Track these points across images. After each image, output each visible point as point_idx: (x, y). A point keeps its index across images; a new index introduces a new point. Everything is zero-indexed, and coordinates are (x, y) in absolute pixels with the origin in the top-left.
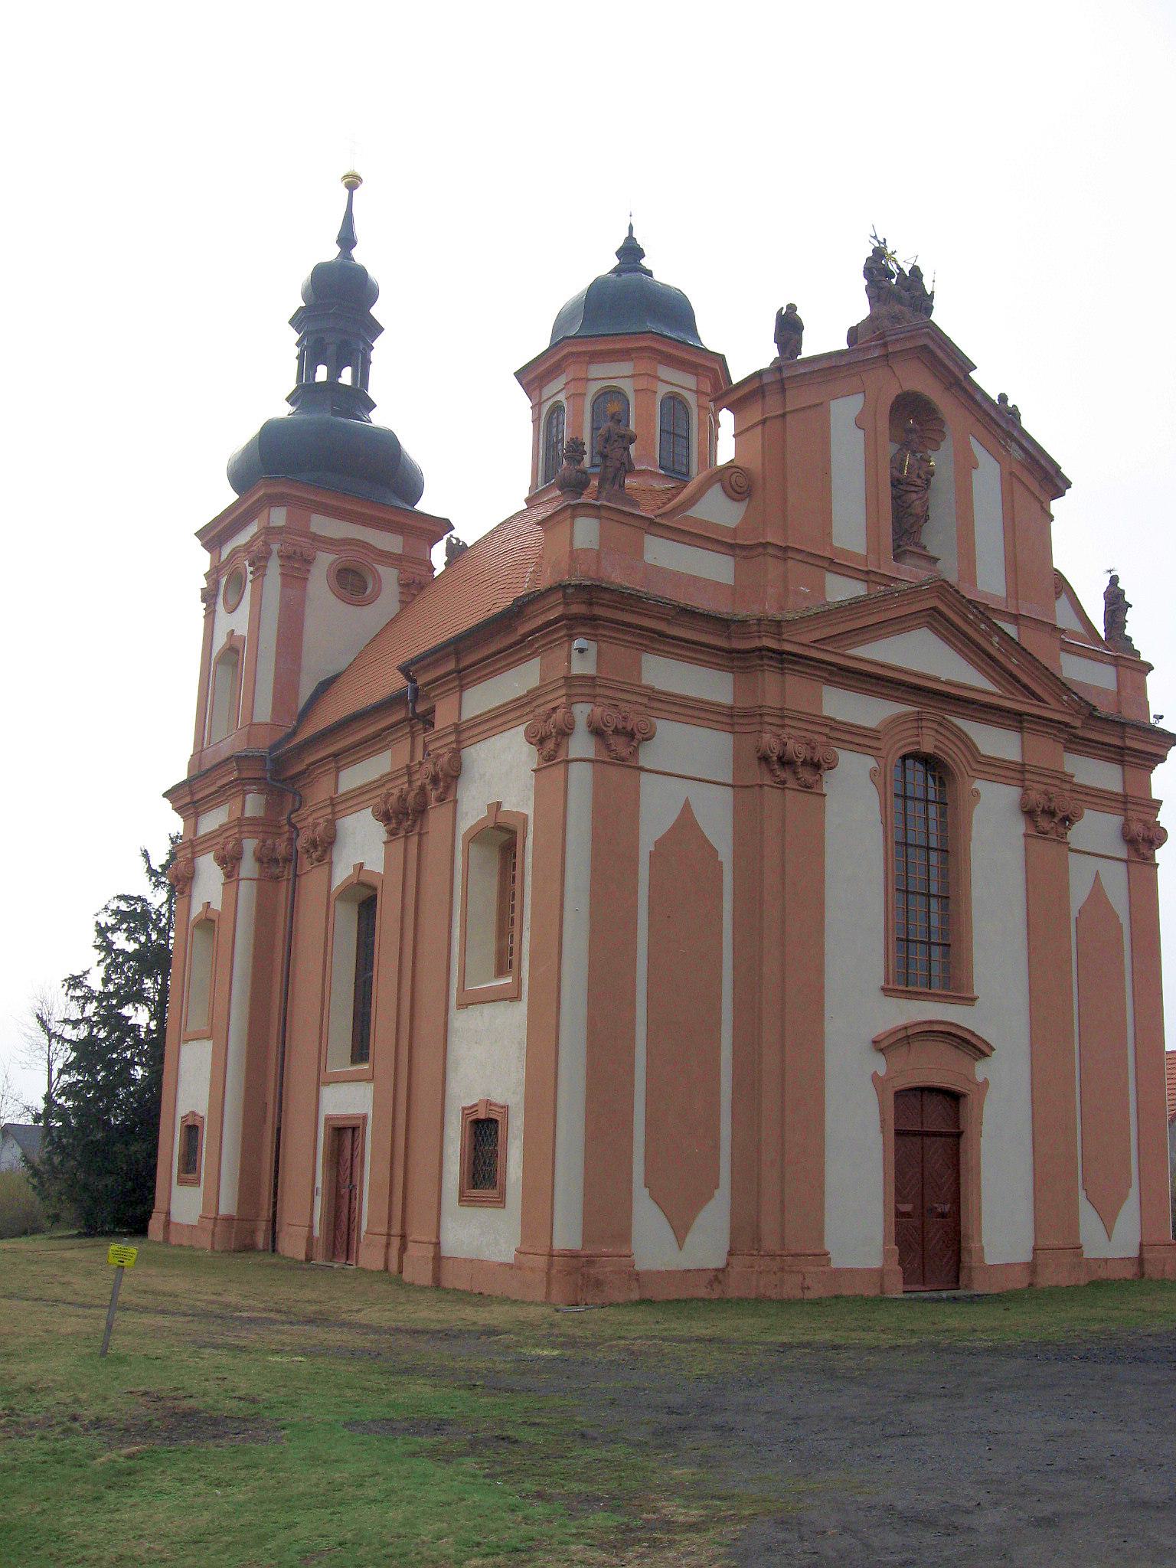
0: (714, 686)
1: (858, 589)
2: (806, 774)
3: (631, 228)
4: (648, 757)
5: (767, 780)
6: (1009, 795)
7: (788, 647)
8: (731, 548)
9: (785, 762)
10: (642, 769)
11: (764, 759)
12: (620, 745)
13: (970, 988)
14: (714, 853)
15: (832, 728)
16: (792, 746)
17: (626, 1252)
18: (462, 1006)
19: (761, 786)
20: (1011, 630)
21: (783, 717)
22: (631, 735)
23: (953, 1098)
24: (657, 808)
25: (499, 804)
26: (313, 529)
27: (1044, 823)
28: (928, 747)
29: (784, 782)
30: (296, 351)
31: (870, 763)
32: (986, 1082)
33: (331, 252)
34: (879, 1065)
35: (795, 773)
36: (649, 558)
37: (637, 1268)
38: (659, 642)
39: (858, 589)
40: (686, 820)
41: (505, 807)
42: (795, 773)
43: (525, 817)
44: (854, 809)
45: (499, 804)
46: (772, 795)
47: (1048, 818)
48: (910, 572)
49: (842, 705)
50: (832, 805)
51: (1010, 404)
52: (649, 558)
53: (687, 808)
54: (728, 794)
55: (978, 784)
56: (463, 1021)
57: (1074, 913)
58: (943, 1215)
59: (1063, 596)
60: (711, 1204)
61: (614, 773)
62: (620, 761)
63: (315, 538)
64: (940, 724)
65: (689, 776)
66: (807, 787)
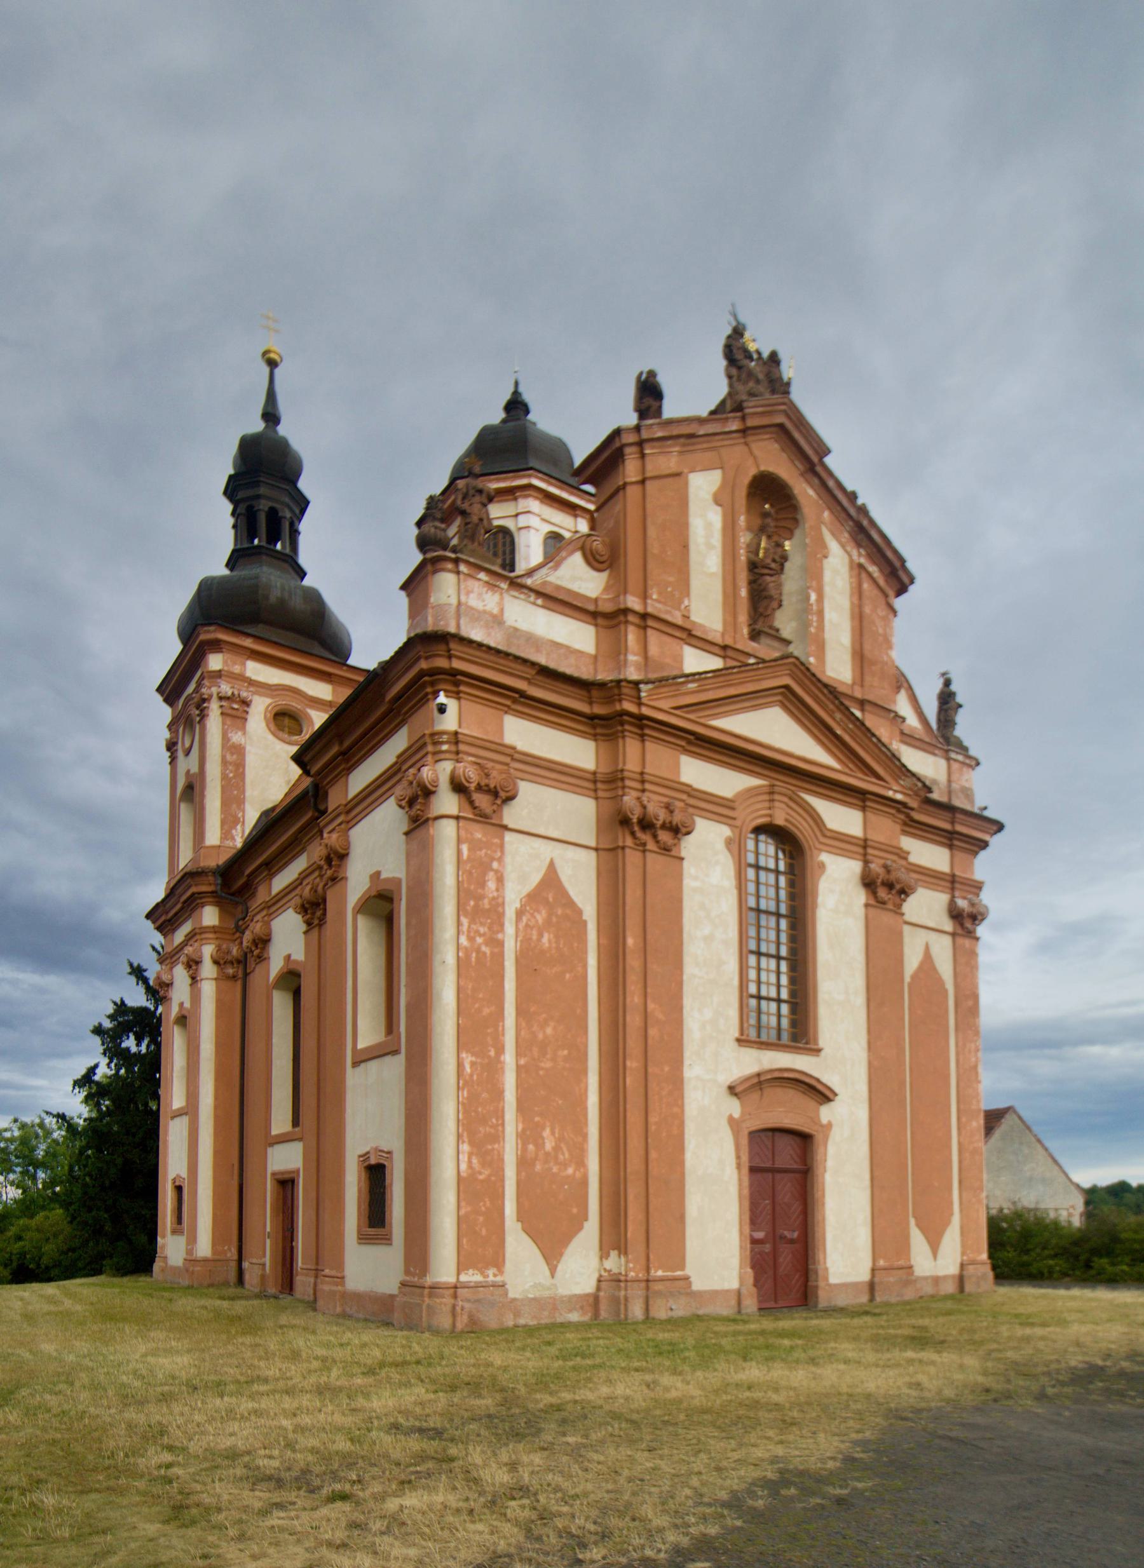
2: (665, 836)
5: (629, 841)
9: (646, 824)
10: (506, 828)
11: (625, 822)
14: (580, 912)
15: (689, 795)
16: (652, 808)
17: (499, 1279)
18: (355, 1064)
19: (623, 848)
21: (643, 782)
24: (521, 865)
25: (378, 873)
26: (249, 674)
29: (644, 844)
30: (232, 521)
35: (655, 836)
37: (511, 1295)
40: (551, 878)
41: (384, 876)
42: (655, 836)
43: (399, 880)
44: (710, 874)
45: (378, 873)
46: (632, 857)
49: (698, 773)
50: (689, 869)
53: (552, 865)
54: (593, 855)
56: (354, 1078)
60: (581, 1235)
63: (251, 683)
64: (791, 798)
65: (550, 839)
66: (666, 850)
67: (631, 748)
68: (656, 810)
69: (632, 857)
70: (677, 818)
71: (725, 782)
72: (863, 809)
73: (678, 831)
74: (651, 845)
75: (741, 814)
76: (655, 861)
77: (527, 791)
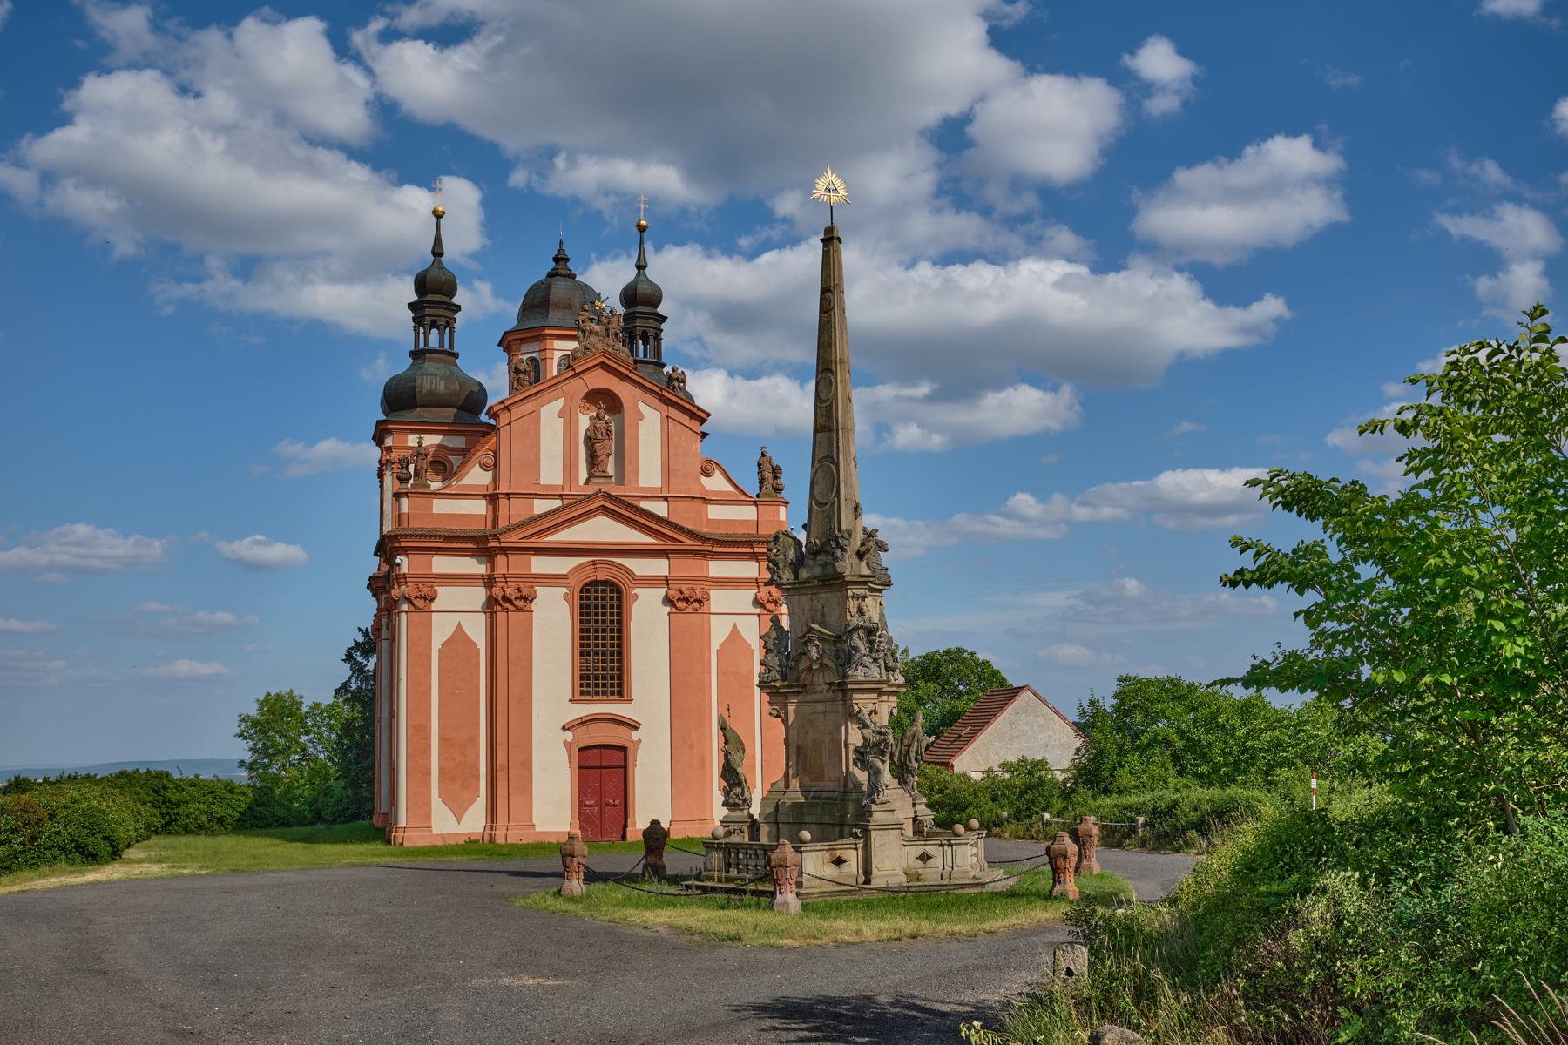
0: (472, 566)
1: (557, 503)
2: (519, 603)
4: (434, 606)
6: (662, 592)
8: (484, 496)
9: (506, 599)
12: (420, 603)
20: (660, 508)
22: (425, 598)
23: (624, 749)
27: (681, 605)
28: (602, 577)
31: (565, 590)
34: (569, 736)
36: (435, 510)
38: (439, 551)
39: (557, 503)
47: (686, 602)
48: (590, 490)
49: (540, 565)
52: (435, 510)
55: (637, 591)
57: (715, 646)
61: (417, 616)
62: (419, 610)
66: (519, 609)
67: (501, 560)
68: (511, 592)
69: (501, 617)
70: (525, 592)
73: (528, 599)
74: (511, 608)
77: (442, 591)
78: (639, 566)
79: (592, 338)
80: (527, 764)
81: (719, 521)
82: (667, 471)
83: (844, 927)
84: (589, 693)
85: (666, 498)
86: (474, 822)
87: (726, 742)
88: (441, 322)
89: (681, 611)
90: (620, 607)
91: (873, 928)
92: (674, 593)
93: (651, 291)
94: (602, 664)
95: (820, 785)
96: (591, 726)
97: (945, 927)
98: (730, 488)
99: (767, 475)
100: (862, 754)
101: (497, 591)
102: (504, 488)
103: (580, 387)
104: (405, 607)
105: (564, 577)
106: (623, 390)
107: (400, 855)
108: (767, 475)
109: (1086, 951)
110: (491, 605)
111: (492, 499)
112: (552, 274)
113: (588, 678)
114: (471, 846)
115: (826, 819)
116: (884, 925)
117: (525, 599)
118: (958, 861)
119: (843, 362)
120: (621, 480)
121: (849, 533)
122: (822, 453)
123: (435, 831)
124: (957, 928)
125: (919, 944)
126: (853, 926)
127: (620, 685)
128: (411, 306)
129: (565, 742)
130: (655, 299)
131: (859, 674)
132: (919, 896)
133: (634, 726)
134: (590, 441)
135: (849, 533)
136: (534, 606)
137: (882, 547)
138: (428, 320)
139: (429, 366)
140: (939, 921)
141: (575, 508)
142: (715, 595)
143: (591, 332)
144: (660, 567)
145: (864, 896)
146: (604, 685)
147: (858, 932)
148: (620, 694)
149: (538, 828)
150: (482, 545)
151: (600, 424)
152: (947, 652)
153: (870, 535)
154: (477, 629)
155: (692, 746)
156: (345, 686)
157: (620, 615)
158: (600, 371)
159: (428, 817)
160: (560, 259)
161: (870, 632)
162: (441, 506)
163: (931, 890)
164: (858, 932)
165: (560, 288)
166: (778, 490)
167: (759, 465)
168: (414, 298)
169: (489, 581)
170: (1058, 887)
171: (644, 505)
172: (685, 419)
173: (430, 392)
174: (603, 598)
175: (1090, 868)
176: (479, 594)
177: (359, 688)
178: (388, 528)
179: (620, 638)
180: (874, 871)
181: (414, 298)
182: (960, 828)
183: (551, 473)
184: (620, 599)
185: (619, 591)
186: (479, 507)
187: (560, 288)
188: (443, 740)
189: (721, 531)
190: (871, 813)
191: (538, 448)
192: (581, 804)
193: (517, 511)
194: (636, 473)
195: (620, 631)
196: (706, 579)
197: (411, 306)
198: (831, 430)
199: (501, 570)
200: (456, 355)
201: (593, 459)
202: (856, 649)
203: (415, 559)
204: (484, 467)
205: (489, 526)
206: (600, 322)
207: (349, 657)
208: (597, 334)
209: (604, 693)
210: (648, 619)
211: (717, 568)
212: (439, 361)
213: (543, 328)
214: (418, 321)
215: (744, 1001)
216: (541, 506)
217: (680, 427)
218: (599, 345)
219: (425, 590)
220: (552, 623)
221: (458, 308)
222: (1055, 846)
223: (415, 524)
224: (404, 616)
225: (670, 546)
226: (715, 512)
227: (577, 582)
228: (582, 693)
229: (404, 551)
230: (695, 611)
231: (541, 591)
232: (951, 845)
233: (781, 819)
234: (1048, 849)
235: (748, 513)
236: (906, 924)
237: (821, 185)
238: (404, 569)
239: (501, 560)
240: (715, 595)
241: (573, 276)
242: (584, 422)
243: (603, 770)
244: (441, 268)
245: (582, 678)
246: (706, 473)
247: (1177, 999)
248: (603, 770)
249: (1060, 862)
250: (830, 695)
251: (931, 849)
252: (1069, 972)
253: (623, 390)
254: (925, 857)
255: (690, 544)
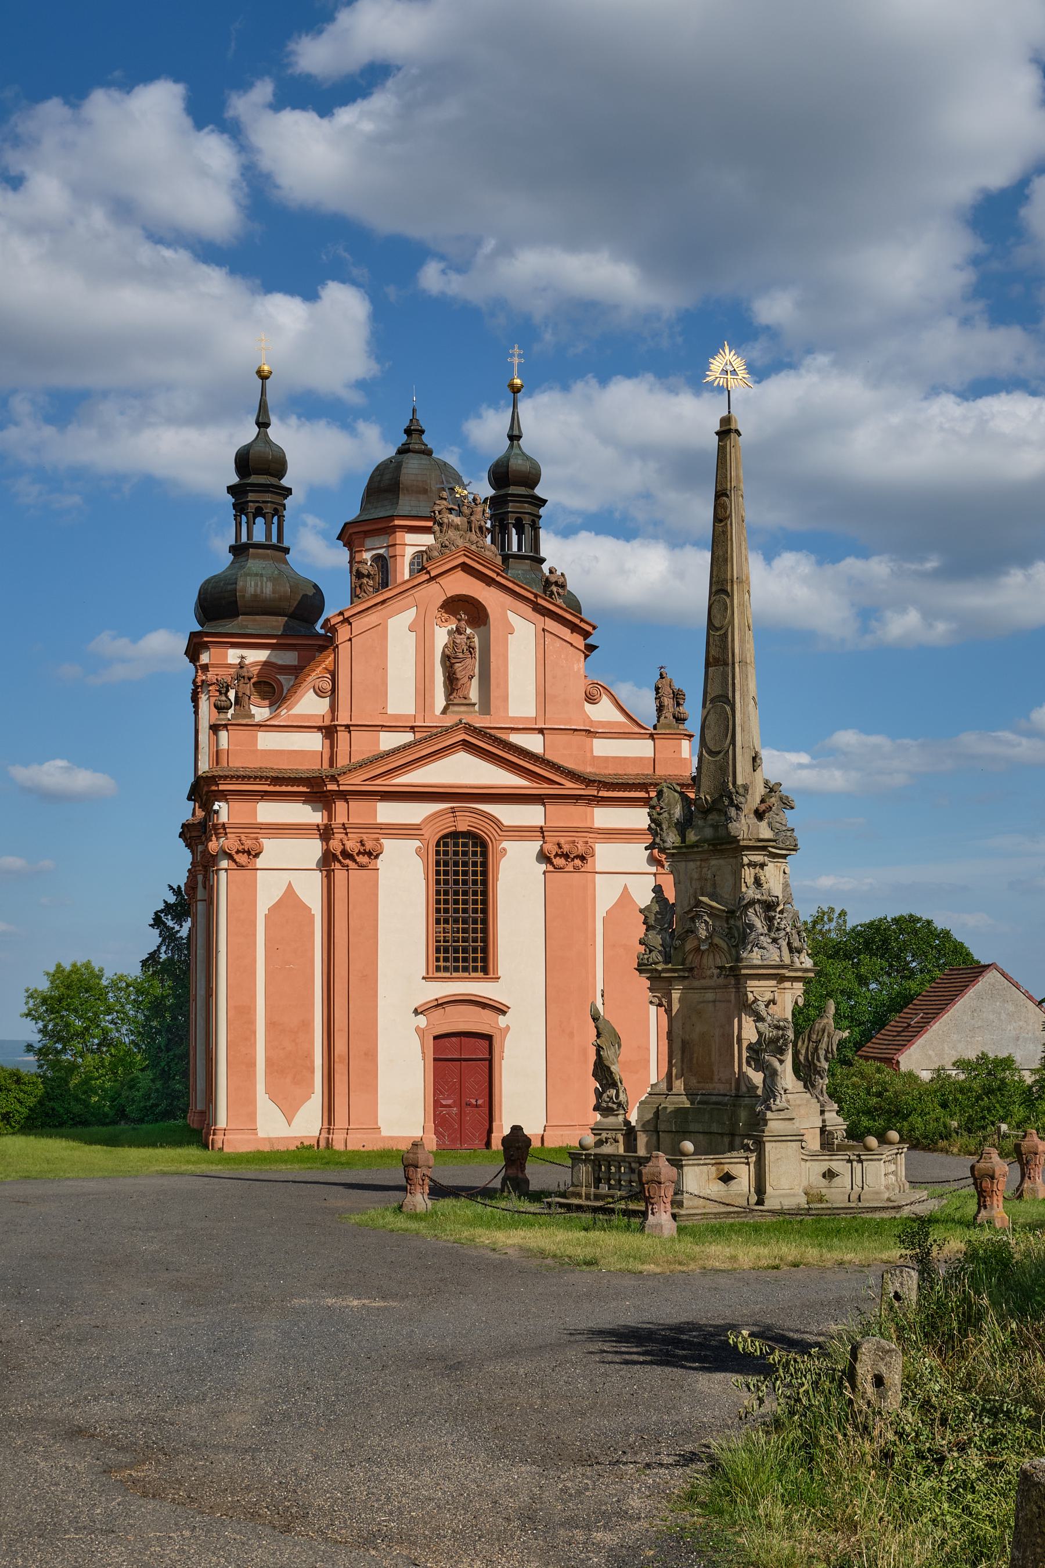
1: (408, 737)
2: (363, 859)
3: (414, 411)
4: (260, 863)
7: (342, 788)
8: (319, 728)
9: (346, 854)
12: (242, 859)
13: (495, 971)
20: (533, 743)
22: (249, 853)
23: (489, 1038)
24: (268, 890)
27: (560, 862)
28: (463, 827)
32: (508, 1028)
33: (248, 433)
34: (422, 1021)
36: (261, 746)
39: (408, 737)
42: (355, 861)
47: (564, 857)
48: (449, 721)
49: (388, 812)
51: (559, 573)
52: (261, 746)
55: (505, 844)
57: (601, 912)
58: (477, 1106)
59: (604, 697)
62: (241, 867)
66: (362, 867)
67: (340, 806)
68: (352, 845)
69: (340, 875)
70: (369, 845)
71: (415, 813)
72: (544, 804)
73: (373, 855)
74: (352, 865)
75: (427, 832)
76: (356, 875)
78: (508, 814)
79: (451, 533)
80: (371, 1055)
81: (606, 759)
82: (543, 697)
83: (718, 1253)
84: (446, 969)
85: (541, 731)
86: (307, 1124)
87: (598, 1036)
88: (268, 509)
89: (558, 869)
90: (484, 864)
91: (749, 1254)
92: (551, 848)
93: (526, 467)
94: (463, 935)
95: (709, 1087)
96: (449, 1009)
97: (832, 1256)
98: (621, 718)
99: (668, 701)
100: (757, 1052)
101: (335, 845)
102: (343, 719)
103: (435, 594)
104: (224, 864)
105: (417, 827)
106: (489, 597)
107: (220, 1161)
108: (668, 701)
109: (914, 1274)
110: (327, 861)
111: (329, 732)
112: (403, 451)
113: (446, 951)
114: (303, 1153)
115: (715, 1128)
116: (764, 1251)
117: (369, 854)
118: (870, 1180)
119: (740, 581)
120: (485, 706)
121: (746, 788)
122: (715, 691)
123: (261, 1134)
124: (849, 1257)
125: (800, 1274)
126: (728, 1251)
127: (485, 960)
128: (231, 489)
129: (417, 1029)
130: (532, 479)
131: (755, 957)
132: (817, 1220)
133: (501, 1010)
134: (449, 661)
135: (746, 788)
136: (380, 863)
137: (787, 804)
138: (251, 508)
139: (254, 565)
140: (830, 1249)
141: (430, 744)
142: (600, 849)
143: (450, 525)
144: (532, 815)
145: (756, 1219)
146: (465, 960)
147: (734, 1258)
148: (485, 970)
149: (385, 1133)
150: (317, 789)
151: (461, 639)
152: (896, 921)
153: (772, 789)
154: (310, 890)
155: (571, 1035)
156: (153, 956)
157: (485, 873)
158: (460, 574)
159: (252, 1116)
160: (413, 431)
161: (769, 906)
162: (267, 741)
163: (834, 1212)
164: (734, 1258)
165: (413, 465)
166: (680, 719)
167: (657, 689)
168: (235, 479)
169: (325, 833)
170: (983, 1213)
171: (515, 739)
172: (565, 633)
173: (255, 596)
174: (465, 853)
175: (1034, 1191)
176: (314, 848)
177: (170, 960)
178: (204, 767)
179: (485, 902)
180: (769, 1190)
181: (235, 479)
182: (872, 1141)
183: (401, 701)
184: (484, 854)
185: (484, 845)
186: (314, 742)
187: (413, 465)
188: (270, 1025)
189: (608, 772)
190: (765, 1122)
191: (385, 669)
192: (437, 1104)
193: (356, 747)
194: (505, 699)
195: (485, 893)
196: (591, 830)
197: (231, 489)
198: (726, 664)
199: (340, 818)
200: (287, 551)
201: (452, 682)
202: (751, 927)
203: (237, 806)
204: (319, 693)
205: (326, 765)
206: (460, 513)
207: (157, 921)
208: (457, 528)
209: (465, 969)
210: (518, 881)
211: (605, 817)
212: (265, 557)
213: (392, 518)
214: (240, 508)
215: (582, 1326)
216: (388, 741)
217: (559, 643)
218: (460, 542)
219: (248, 844)
220: (402, 885)
221: (288, 491)
222: (981, 1165)
223: (237, 763)
224: (223, 875)
225: (545, 789)
226: (602, 748)
227: (433, 834)
228: (438, 969)
229: (223, 796)
230: (577, 869)
231: (390, 846)
232: (860, 1161)
233: (662, 1127)
234: (972, 1168)
235: (643, 748)
236: (789, 1250)
237: (717, 365)
238: (223, 818)
239: (340, 806)
240: (600, 849)
241: (428, 453)
242: (441, 637)
243: (464, 1062)
244: (268, 442)
245: (438, 951)
246: (591, 699)
247: (1004, 1328)
248: (464, 1062)
249: (986, 1183)
250: (721, 981)
251: (838, 1165)
252: (897, 1297)
253: (489, 597)
254: (829, 1175)
255: (570, 787)
